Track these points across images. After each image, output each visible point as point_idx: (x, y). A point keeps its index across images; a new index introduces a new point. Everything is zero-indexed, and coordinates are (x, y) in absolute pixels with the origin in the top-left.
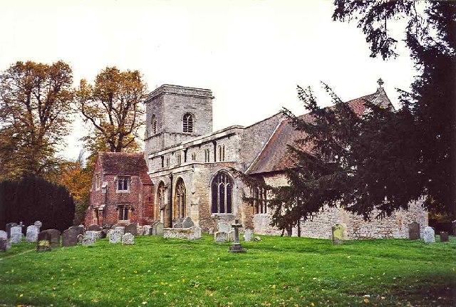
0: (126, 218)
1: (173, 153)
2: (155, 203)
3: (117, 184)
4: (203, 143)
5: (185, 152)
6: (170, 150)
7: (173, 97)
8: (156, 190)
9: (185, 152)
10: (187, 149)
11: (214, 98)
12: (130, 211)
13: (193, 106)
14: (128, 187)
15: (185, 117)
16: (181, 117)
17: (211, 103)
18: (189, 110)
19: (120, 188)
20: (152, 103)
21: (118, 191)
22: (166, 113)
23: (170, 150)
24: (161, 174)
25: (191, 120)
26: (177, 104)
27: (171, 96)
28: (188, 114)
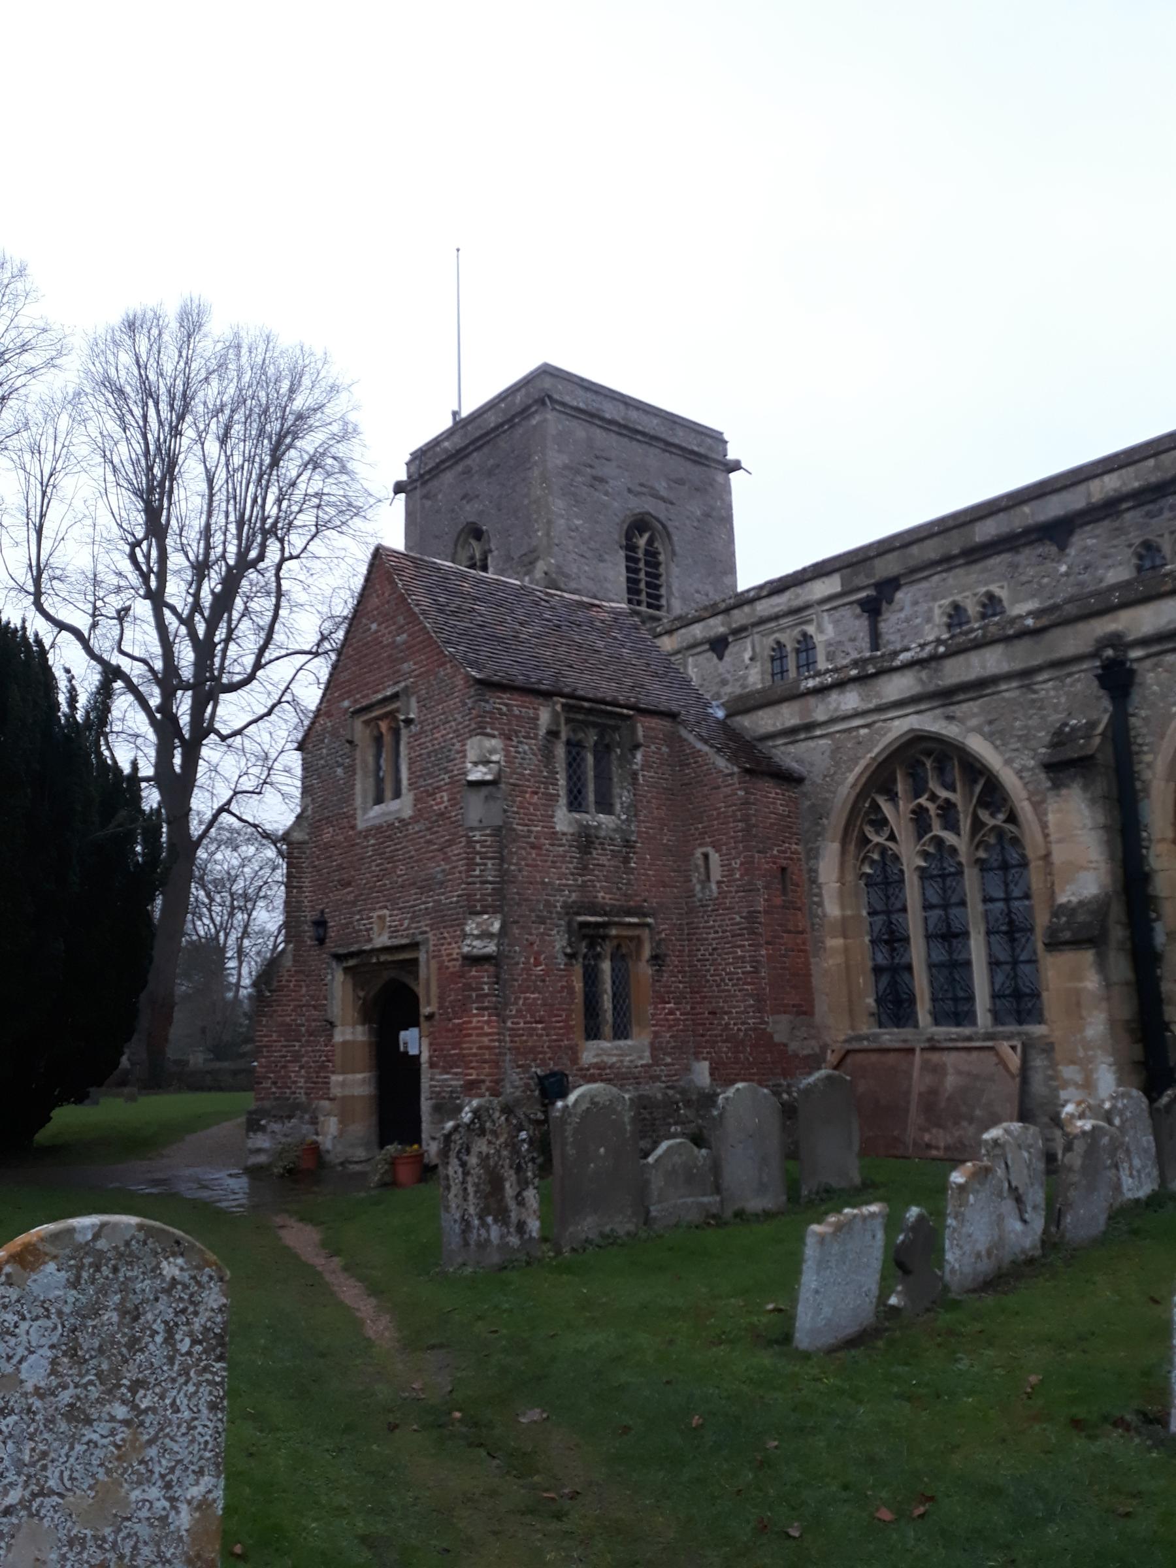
0: (621, 1032)
1: (718, 645)
2: (832, 909)
3: (560, 751)
4: (1109, 508)
5: (873, 609)
6: (697, 631)
7: (580, 431)
8: (836, 820)
9: (873, 609)
10: (887, 588)
11: (736, 466)
12: (644, 970)
13: (662, 487)
14: (622, 797)
15: (629, 536)
16: (618, 536)
17: (727, 489)
18: (648, 505)
19: (576, 803)
20: (448, 477)
21: (563, 820)
22: (558, 505)
23: (697, 631)
24: (898, 686)
25: (652, 554)
26: (598, 472)
27: (574, 424)
28: (640, 524)
